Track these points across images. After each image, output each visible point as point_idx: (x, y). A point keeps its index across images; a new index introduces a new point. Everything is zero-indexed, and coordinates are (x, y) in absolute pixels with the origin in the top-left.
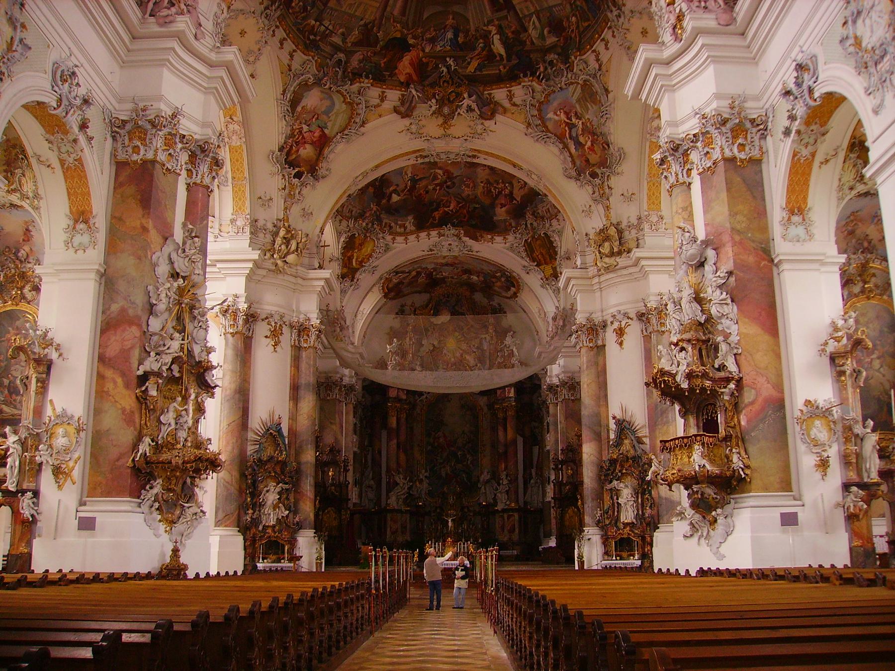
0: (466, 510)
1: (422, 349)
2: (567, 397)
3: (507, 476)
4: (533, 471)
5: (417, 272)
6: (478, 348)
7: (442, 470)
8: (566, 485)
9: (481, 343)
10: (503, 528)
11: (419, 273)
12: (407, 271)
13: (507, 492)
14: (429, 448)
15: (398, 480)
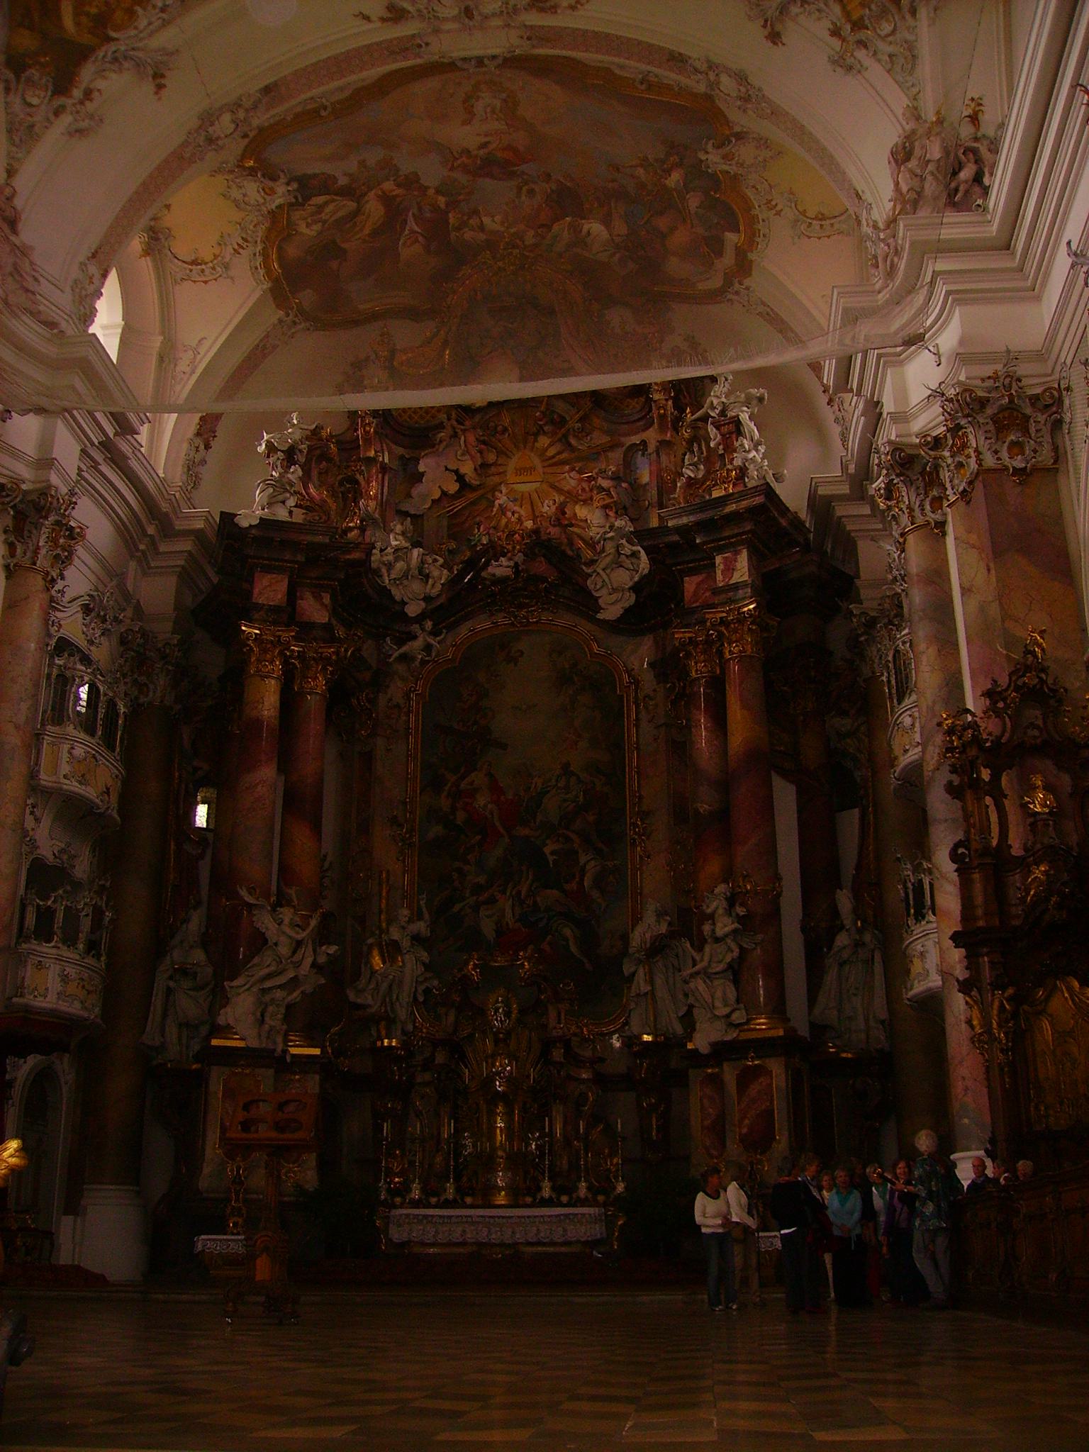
0: (558, 1054)
1: (418, 490)
2: (989, 461)
3: (731, 901)
4: (844, 901)
5: (386, 199)
6: (616, 478)
7: (483, 913)
8: (1023, 864)
9: (628, 463)
10: (718, 1129)
11: (394, 212)
12: (343, 181)
13: (736, 972)
14: (436, 830)
15: (266, 922)
